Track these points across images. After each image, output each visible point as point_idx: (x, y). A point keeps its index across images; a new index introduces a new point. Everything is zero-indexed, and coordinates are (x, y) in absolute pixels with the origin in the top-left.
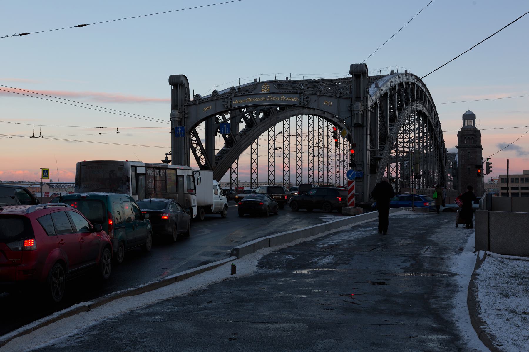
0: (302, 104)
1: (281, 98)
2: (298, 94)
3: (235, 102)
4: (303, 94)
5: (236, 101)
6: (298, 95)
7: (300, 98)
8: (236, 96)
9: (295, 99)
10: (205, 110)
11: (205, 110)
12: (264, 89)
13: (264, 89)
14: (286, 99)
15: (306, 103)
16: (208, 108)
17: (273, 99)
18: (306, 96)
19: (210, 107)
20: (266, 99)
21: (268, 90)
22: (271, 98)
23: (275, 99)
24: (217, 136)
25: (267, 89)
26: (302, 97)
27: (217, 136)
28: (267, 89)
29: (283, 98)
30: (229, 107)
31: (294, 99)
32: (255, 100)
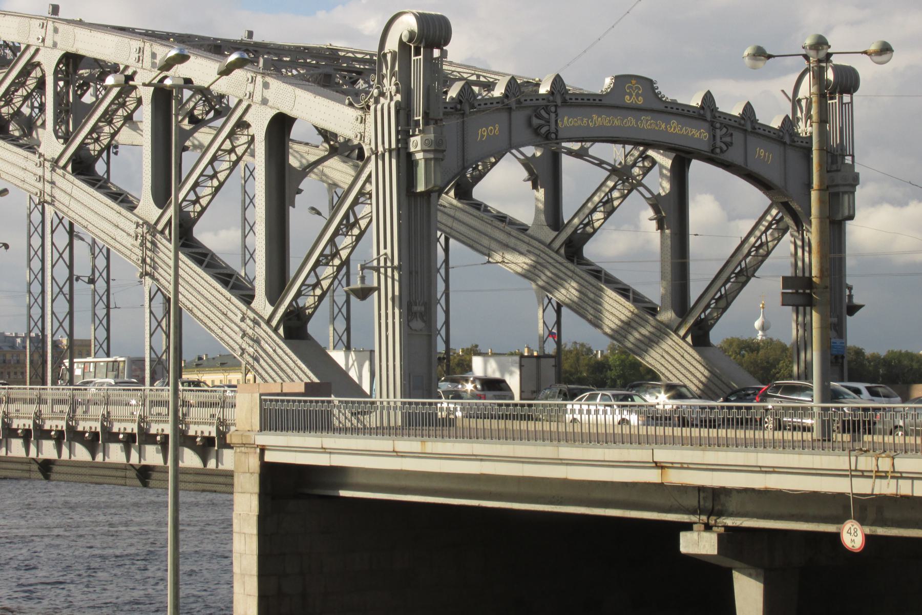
0: (718, 150)
1: (671, 127)
2: (706, 120)
3: (562, 121)
4: (721, 124)
5: (566, 119)
6: (707, 125)
7: (714, 136)
8: (565, 103)
9: (700, 134)
10: (482, 136)
11: (482, 136)
12: (631, 95)
13: (631, 95)
14: (681, 130)
15: (724, 148)
16: (491, 131)
17: (651, 124)
18: (724, 130)
19: (495, 129)
20: (637, 123)
21: (640, 98)
22: (647, 123)
23: (657, 125)
24: (294, 207)
25: (638, 95)
26: (719, 133)
27: (294, 207)
28: (638, 95)
29: (675, 128)
30: (553, 136)
31: (698, 134)
32: (610, 121)
